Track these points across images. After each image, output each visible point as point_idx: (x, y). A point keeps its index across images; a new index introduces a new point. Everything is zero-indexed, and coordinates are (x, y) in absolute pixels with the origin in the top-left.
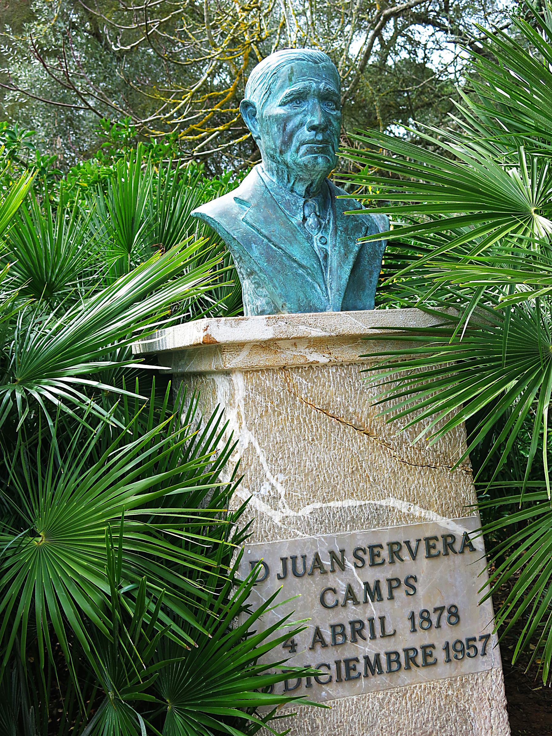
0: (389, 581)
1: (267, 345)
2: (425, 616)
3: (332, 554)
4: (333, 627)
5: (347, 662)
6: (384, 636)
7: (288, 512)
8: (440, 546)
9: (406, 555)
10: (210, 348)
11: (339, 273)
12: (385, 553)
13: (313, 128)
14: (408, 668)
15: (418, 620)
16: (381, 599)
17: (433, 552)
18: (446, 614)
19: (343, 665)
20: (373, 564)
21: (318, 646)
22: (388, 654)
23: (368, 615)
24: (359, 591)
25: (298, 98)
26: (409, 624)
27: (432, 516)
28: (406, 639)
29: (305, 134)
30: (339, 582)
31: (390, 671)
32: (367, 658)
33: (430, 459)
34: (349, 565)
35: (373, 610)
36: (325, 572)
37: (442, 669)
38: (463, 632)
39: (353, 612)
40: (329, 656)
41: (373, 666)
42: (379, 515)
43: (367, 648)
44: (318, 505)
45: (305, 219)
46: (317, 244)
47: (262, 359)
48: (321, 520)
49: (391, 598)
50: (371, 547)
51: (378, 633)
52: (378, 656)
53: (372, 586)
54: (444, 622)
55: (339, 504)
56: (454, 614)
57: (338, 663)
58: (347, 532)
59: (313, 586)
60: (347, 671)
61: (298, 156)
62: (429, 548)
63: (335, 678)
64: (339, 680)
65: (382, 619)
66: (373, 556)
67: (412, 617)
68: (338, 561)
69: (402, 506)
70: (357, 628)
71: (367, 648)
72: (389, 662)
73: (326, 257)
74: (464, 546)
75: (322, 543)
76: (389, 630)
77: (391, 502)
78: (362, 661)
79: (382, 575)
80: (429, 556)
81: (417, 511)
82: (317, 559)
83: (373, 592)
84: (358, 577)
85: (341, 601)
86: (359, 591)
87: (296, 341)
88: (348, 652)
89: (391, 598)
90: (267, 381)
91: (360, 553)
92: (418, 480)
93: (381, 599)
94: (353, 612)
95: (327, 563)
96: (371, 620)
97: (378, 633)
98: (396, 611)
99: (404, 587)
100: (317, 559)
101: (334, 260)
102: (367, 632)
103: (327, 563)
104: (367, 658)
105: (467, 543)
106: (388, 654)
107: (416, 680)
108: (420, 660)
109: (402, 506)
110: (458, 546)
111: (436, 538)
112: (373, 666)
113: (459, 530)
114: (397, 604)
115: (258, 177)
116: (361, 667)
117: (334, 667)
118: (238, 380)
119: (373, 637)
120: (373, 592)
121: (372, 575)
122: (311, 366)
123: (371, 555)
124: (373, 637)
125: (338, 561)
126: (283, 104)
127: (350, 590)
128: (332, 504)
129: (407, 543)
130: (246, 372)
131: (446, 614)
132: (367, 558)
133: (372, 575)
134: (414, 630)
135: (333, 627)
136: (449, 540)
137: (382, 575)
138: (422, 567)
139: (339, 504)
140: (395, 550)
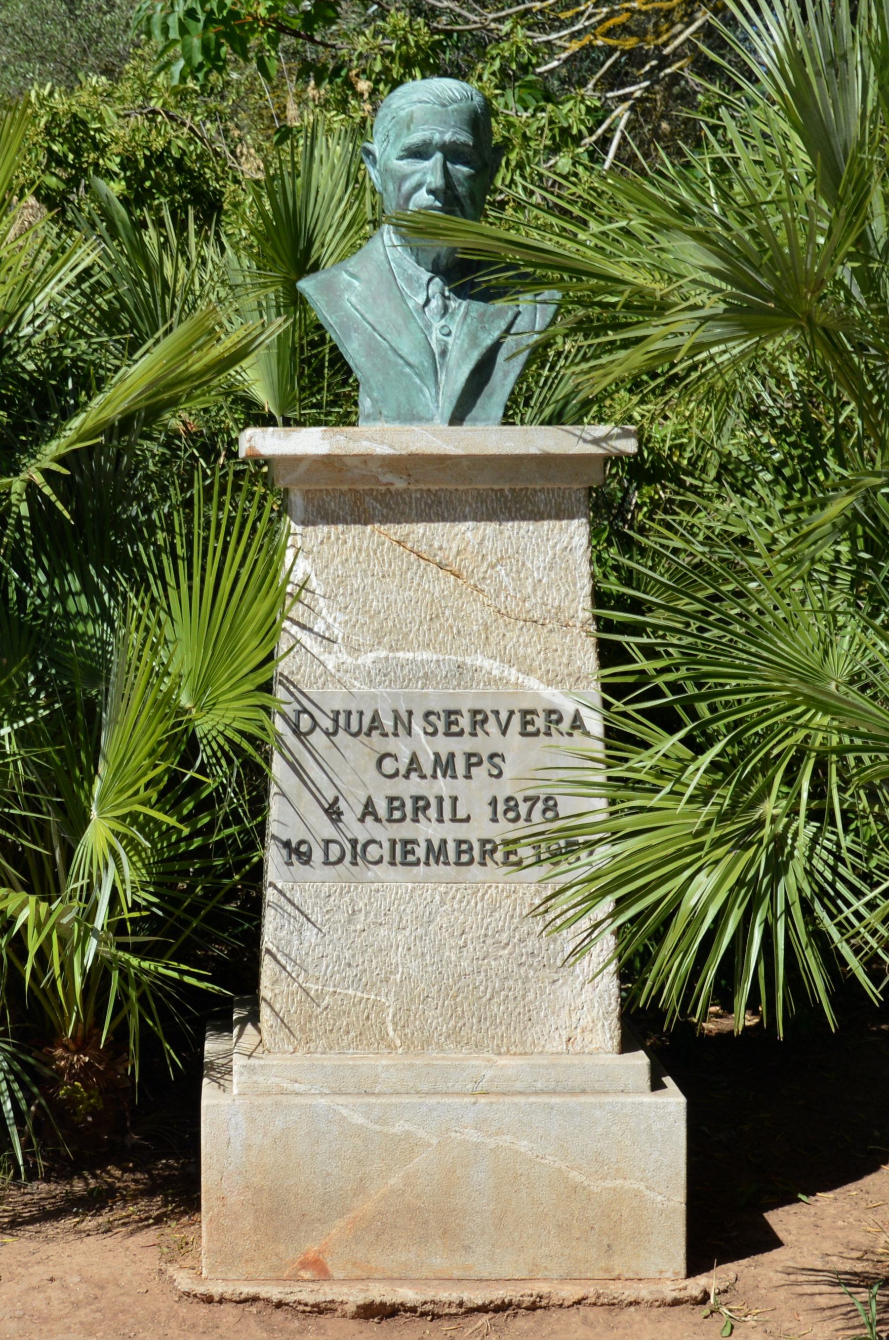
0: (469, 756)
3: (397, 717)
4: (391, 799)
5: (405, 842)
6: (454, 820)
7: (344, 657)
8: (540, 722)
9: (492, 726)
12: (465, 722)
13: (430, 192)
14: (483, 864)
15: (501, 807)
16: (454, 777)
17: (530, 728)
18: (540, 806)
19: (398, 847)
20: (448, 734)
21: (369, 819)
22: (459, 843)
23: (436, 791)
26: (489, 809)
27: (533, 683)
28: (482, 827)
30: (402, 748)
31: (458, 863)
32: (429, 842)
33: (536, 615)
34: (417, 729)
35: (443, 786)
36: (385, 735)
39: (413, 786)
40: (383, 833)
41: (437, 853)
43: (428, 830)
44: (383, 654)
45: (428, 301)
46: (435, 336)
48: (384, 672)
49: (468, 776)
50: (449, 713)
51: (447, 814)
52: (444, 842)
53: (444, 759)
54: (536, 816)
55: (410, 655)
57: (393, 843)
58: (416, 689)
60: (403, 853)
62: (525, 724)
63: (387, 858)
64: (393, 863)
65: (455, 799)
66: (449, 724)
67: (494, 802)
68: (403, 723)
69: (494, 667)
70: (420, 805)
71: (428, 830)
72: (459, 853)
73: (444, 353)
74: (574, 727)
75: (384, 700)
76: (461, 814)
77: (480, 661)
78: (423, 845)
79: (460, 746)
80: (524, 734)
81: (513, 674)
82: (375, 718)
84: (428, 749)
85: (403, 771)
89: (468, 776)
91: (432, 718)
93: (454, 777)
94: (413, 786)
95: (388, 723)
96: (440, 800)
97: (447, 814)
98: (474, 792)
99: (486, 764)
100: (375, 718)
102: (432, 812)
103: (388, 723)
104: (429, 842)
105: (577, 723)
106: (459, 843)
108: (499, 856)
109: (494, 667)
110: (565, 726)
111: (533, 712)
112: (437, 853)
113: (568, 707)
114: (472, 783)
116: (421, 852)
117: (386, 845)
119: (440, 820)
121: (444, 745)
124: (440, 820)
126: (401, 158)
127: (414, 759)
128: (401, 654)
129: (496, 713)
131: (540, 806)
132: (441, 725)
133: (444, 745)
134: (495, 820)
135: (391, 799)
136: (553, 716)
137: (460, 746)
139: (410, 655)
140: (479, 719)
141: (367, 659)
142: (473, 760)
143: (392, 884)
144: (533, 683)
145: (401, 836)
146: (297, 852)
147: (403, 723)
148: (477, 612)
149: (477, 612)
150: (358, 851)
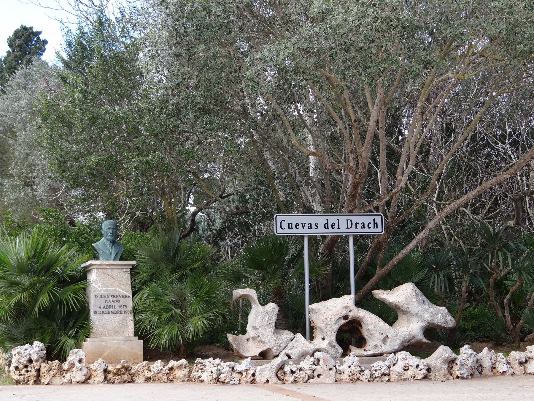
1: (100, 265)
2: (121, 306)
10: (91, 265)
11: (113, 255)
24: (111, 301)
25: (109, 229)
27: (124, 292)
28: (118, 309)
29: (110, 234)
30: (108, 300)
35: (113, 304)
37: (123, 315)
38: (127, 310)
39: (110, 304)
40: (106, 310)
41: (112, 312)
42: (115, 291)
43: (111, 310)
47: (99, 267)
48: (106, 290)
56: (126, 306)
59: (104, 299)
60: (108, 312)
61: (109, 238)
69: (119, 290)
70: (110, 306)
71: (111, 310)
75: (106, 293)
79: (115, 299)
83: (113, 302)
84: (111, 300)
86: (111, 301)
87: (104, 264)
88: (109, 309)
90: (100, 270)
92: (122, 286)
94: (110, 304)
98: (117, 305)
101: (113, 253)
105: (129, 296)
107: (119, 315)
109: (119, 290)
112: (112, 312)
113: (128, 295)
115: (103, 240)
118: (95, 270)
120: (113, 302)
121: (114, 299)
122: (107, 268)
123: (114, 296)
125: (108, 297)
130: (97, 268)
133: (114, 299)
136: (126, 296)
137: (115, 299)
138: (121, 299)
140: (117, 296)
141: (104, 289)
142: (117, 301)
143: (107, 316)
144: (124, 292)
145: (108, 310)
146: (95, 312)
147: (108, 297)
148: (117, 283)
149: (117, 283)
150: (103, 312)
